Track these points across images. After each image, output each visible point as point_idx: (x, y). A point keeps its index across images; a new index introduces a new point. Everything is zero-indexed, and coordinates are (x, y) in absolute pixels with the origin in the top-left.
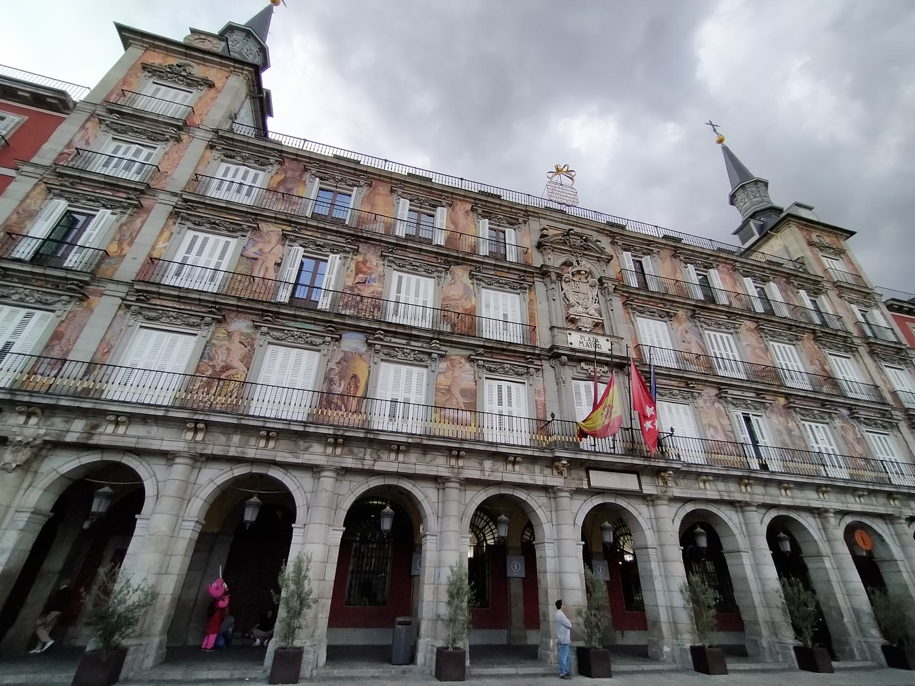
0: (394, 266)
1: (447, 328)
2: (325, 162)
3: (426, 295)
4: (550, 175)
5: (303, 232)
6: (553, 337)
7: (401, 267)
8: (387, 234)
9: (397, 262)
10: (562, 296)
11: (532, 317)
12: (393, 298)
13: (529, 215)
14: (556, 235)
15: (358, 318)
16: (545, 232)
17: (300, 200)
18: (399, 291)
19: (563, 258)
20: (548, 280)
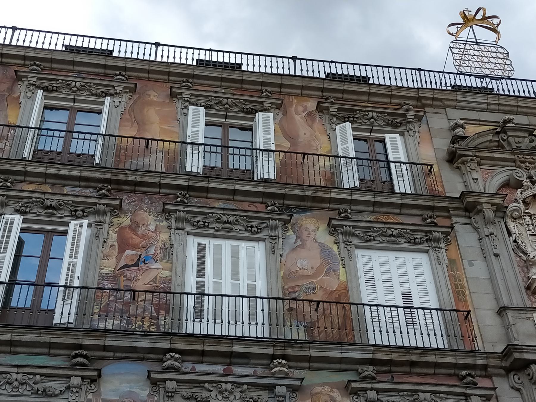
0: (189, 228)
1: (298, 333)
2: (51, 61)
3: (251, 276)
4: (454, 29)
5: (19, 186)
6: (507, 327)
7: (201, 228)
8: (170, 173)
9: (194, 219)
10: (511, 245)
11: (459, 293)
12: (191, 286)
13: (424, 106)
14: (479, 135)
15: (129, 333)
16: (459, 131)
17: (12, 132)
18: (201, 272)
19: (500, 177)
20: (477, 219)
